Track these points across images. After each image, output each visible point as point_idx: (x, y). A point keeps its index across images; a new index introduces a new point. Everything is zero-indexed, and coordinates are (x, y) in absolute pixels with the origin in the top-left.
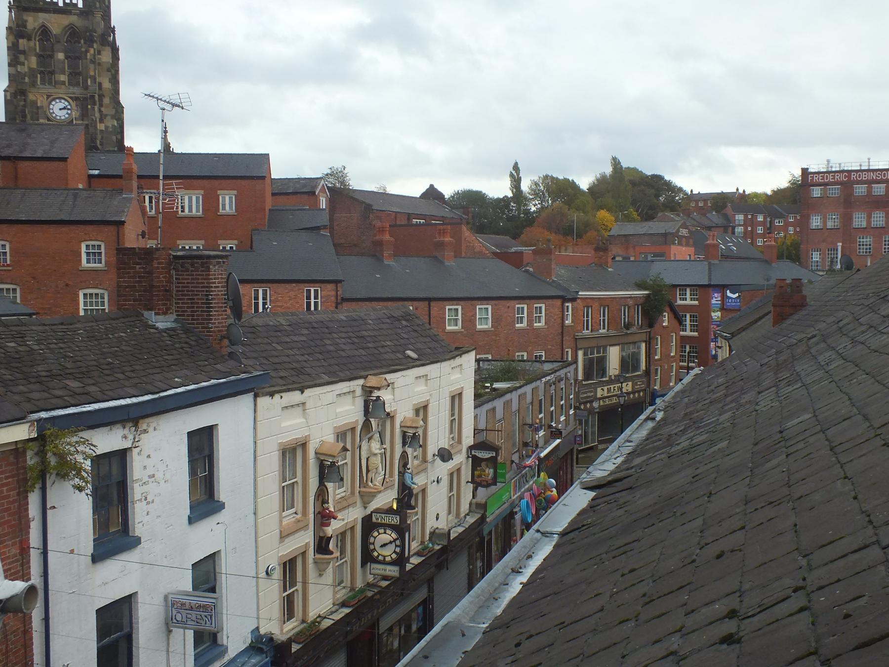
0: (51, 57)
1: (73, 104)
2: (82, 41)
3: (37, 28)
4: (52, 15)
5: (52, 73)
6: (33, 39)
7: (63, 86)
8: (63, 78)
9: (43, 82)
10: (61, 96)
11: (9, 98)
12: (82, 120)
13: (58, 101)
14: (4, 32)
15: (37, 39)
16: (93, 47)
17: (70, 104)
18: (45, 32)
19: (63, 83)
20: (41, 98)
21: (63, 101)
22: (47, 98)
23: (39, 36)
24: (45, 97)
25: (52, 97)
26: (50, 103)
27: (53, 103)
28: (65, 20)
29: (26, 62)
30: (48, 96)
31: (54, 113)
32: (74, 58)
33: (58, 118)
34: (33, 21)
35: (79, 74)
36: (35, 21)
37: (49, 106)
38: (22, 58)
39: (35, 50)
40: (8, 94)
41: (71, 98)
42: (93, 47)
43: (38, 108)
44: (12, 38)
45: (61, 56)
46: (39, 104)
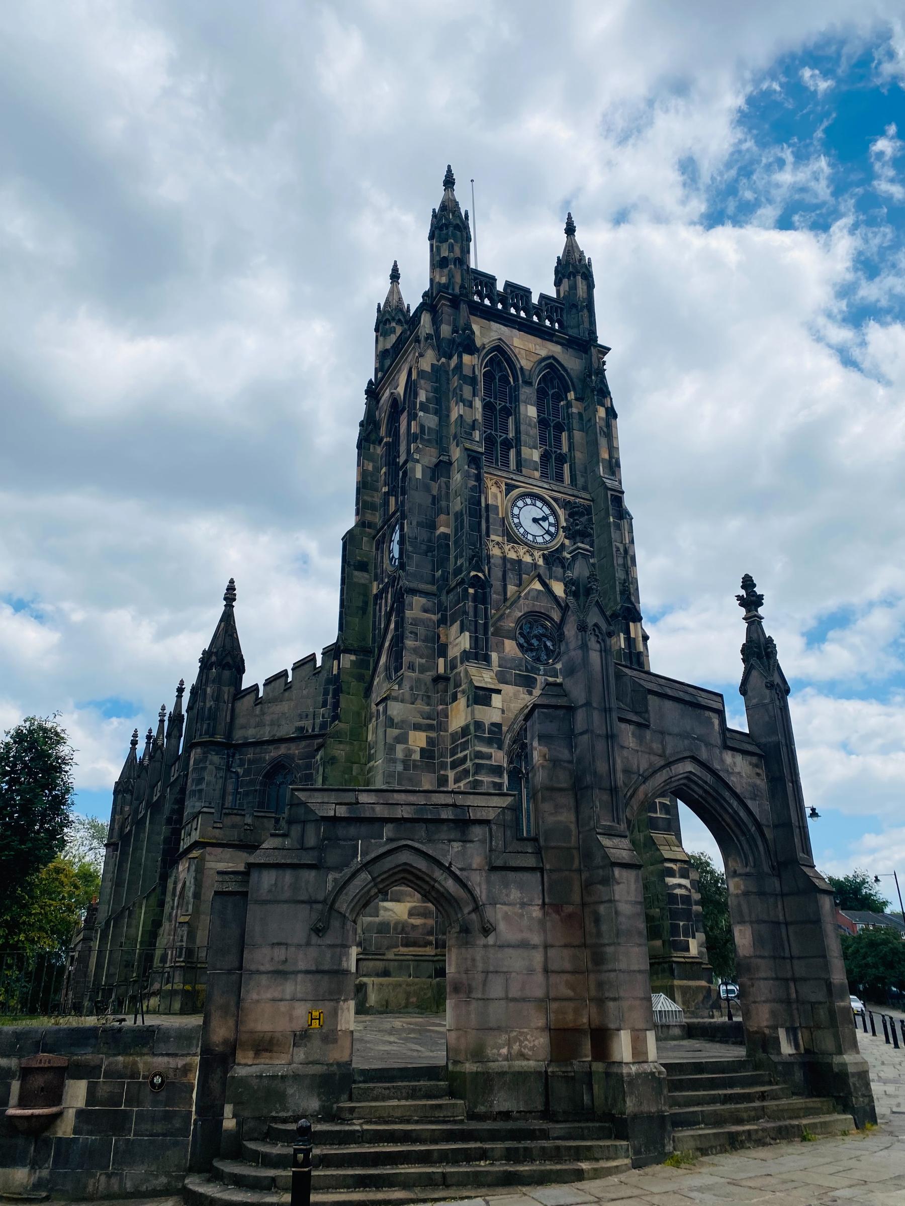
1: (561, 512)
2: (571, 396)
4: (516, 332)
5: (507, 445)
10: (536, 490)
17: (554, 513)
21: (539, 504)
22: (508, 492)
24: (503, 487)
25: (516, 492)
27: (520, 503)
30: (510, 488)
31: (519, 525)
33: (530, 537)
35: (561, 459)
41: (555, 500)
45: (532, 411)
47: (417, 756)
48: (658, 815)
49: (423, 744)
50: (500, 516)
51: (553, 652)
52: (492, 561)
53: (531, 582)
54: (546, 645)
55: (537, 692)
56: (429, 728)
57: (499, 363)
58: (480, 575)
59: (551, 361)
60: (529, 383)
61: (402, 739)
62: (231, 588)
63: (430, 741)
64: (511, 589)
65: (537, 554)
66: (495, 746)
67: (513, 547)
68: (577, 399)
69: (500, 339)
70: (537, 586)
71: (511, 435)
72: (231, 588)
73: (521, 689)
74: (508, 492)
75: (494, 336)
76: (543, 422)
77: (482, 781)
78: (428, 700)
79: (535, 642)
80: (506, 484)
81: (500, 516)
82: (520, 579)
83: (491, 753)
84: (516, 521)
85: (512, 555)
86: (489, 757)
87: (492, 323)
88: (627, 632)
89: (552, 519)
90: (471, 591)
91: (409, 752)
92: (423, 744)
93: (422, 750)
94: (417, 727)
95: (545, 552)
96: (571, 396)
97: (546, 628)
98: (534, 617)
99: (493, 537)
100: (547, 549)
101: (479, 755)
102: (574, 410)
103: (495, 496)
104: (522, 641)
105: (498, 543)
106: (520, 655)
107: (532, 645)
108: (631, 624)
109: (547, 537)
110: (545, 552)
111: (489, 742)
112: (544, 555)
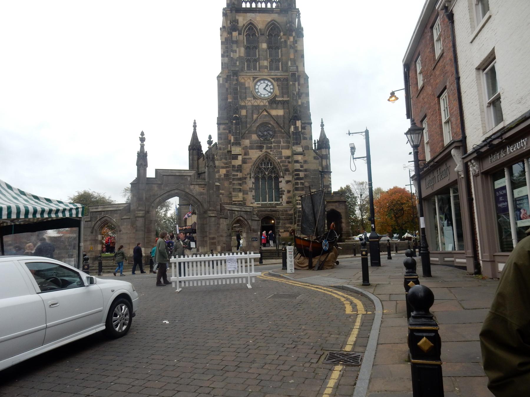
0: (256, 48)
1: (275, 84)
3: (246, 25)
4: (258, 14)
5: (256, 61)
6: (242, 34)
7: (266, 70)
8: (265, 63)
9: (249, 68)
10: (265, 77)
11: (221, 82)
12: (283, 97)
13: (262, 82)
14: (219, 32)
15: (245, 34)
16: (292, 35)
17: (272, 84)
18: (251, 27)
19: (266, 67)
20: (249, 80)
22: (254, 80)
23: (246, 32)
24: (252, 79)
25: (257, 79)
26: (256, 84)
27: (259, 84)
28: (268, 18)
29: (237, 50)
30: (254, 78)
31: (259, 92)
32: (273, 47)
33: (262, 96)
34: (242, 20)
35: (279, 60)
36: (243, 20)
37: (255, 86)
38: (235, 47)
39: (244, 43)
40: (221, 79)
41: (273, 79)
42: (292, 35)
43: (246, 88)
44: (225, 35)
45: (264, 46)
46: (247, 85)
47: (223, 176)
48: (299, 186)
49: (225, 173)
50: (251, 90)
51: (272, 135)
52: (248, 107)
53: (263, 112)
54: (269, 133)
55: (264, 150)
56: (226, 167)
57: (252, 29)
58: (237, 115)
59: (273, 22)
60: (262, 35)
61: (218, 172)
62: (195, 123)
63: (227, 171)
64: (255, 116)
65: (265, 101)
66: (239, 172)
67: (256, 101)
68: (284, 35)
69: (251, 20)
70: (265, 113)
71: (257, 56)
72: (195, 123)
73: (258, 150)
74: (254, 80)
75: (249, 19)
76: (269, 47)
77: (235, 183)
78: (226, 159)
79: (265, 133)
80: (253, 78)
81: (251, 90)
82: (259, 112)
83: (238, 174)
84: (257, 91)
85: (256, 104)
86: (237, 175)
87: (248, 14)
88: (295, 124)
89: (271, 87)
90: (234, 122)
91: (220, 176)
92: (225, 173)
93: (224, 174)
94: (223, 168)
95: (269, 100)
96: (282, 34)
97: (269, 127)
98: (264, 125)
99: (248, 99)
100: (269, 99)
101: (234, 175)
102: (283, 40)
103: (249, 83)
104: (260, 133)
105: (250, 101)
106: (258, 139)
107: (264, 134)
108: (297, 122)
109: (270, 94)
110: (269, 100)
111: (237, 171)
112: (268, 101)
